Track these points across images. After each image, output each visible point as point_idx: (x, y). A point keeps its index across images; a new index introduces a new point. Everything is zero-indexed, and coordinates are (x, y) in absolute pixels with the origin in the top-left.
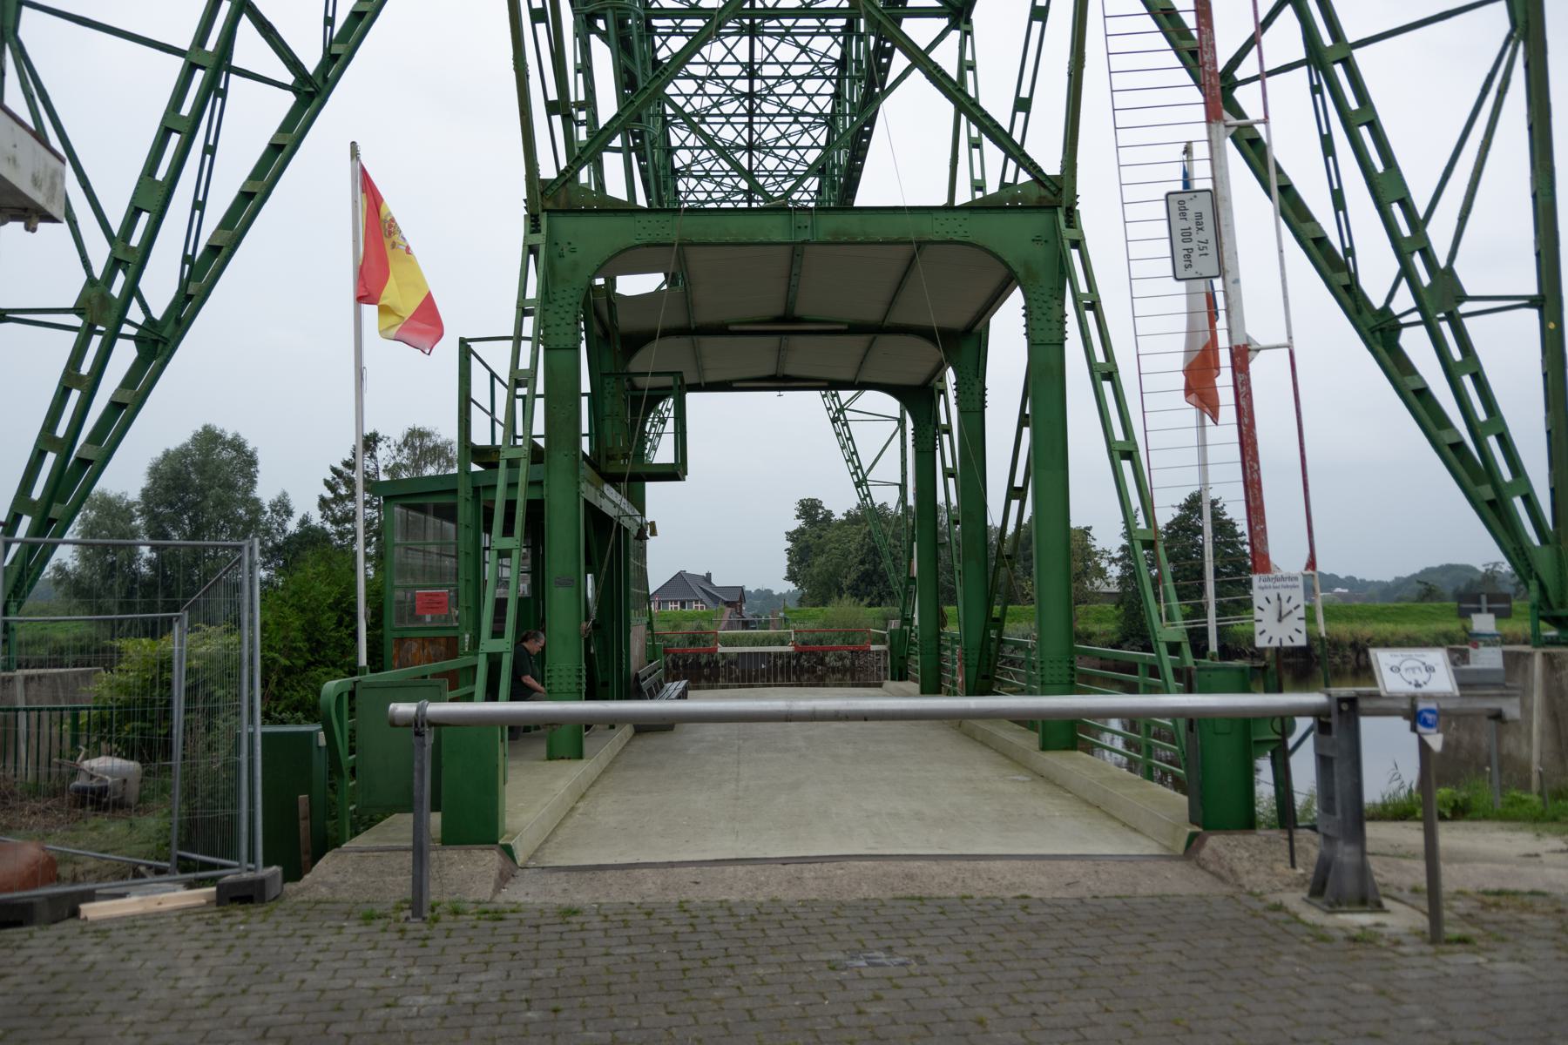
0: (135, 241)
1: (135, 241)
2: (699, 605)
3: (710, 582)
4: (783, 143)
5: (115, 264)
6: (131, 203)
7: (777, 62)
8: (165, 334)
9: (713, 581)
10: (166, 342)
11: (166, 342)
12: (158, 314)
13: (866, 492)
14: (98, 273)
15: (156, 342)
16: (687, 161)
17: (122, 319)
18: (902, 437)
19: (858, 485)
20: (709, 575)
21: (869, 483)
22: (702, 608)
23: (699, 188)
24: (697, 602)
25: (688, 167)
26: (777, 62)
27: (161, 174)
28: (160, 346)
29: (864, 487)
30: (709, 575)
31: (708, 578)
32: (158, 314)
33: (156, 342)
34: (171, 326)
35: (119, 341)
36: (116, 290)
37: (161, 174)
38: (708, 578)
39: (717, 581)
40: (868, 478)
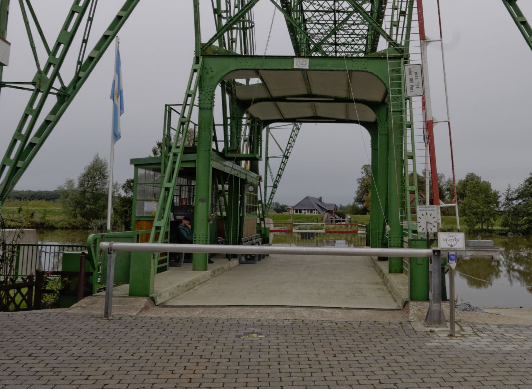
0: (58, 56)
1: (58, 56)
2: (316, 212)
3: (321, 202)
5: (49, 65)
6: (57, 41)
8: (69, 93)
9: (322, 201)
10: (69, 96)
11: (69, 96)
12: (66, 84)
14: (42, 68)
15: (65, 96)
16: (310, 16)
17: (50, 87)
20: (321, 198)
22: (317, 213)
23: (315, 27)
24: (314, 210)
25: (309, 18)
27: (70, 29)
28: (66, 98)
30: (321, 198)
31: (320, 200)
32: (66, 84)
33: (65, 96)
34: (71, 89)
35: (49, 95)
36: (49, 75)
37: (70, 29)
38: (320, 200)
39: (325, 200)
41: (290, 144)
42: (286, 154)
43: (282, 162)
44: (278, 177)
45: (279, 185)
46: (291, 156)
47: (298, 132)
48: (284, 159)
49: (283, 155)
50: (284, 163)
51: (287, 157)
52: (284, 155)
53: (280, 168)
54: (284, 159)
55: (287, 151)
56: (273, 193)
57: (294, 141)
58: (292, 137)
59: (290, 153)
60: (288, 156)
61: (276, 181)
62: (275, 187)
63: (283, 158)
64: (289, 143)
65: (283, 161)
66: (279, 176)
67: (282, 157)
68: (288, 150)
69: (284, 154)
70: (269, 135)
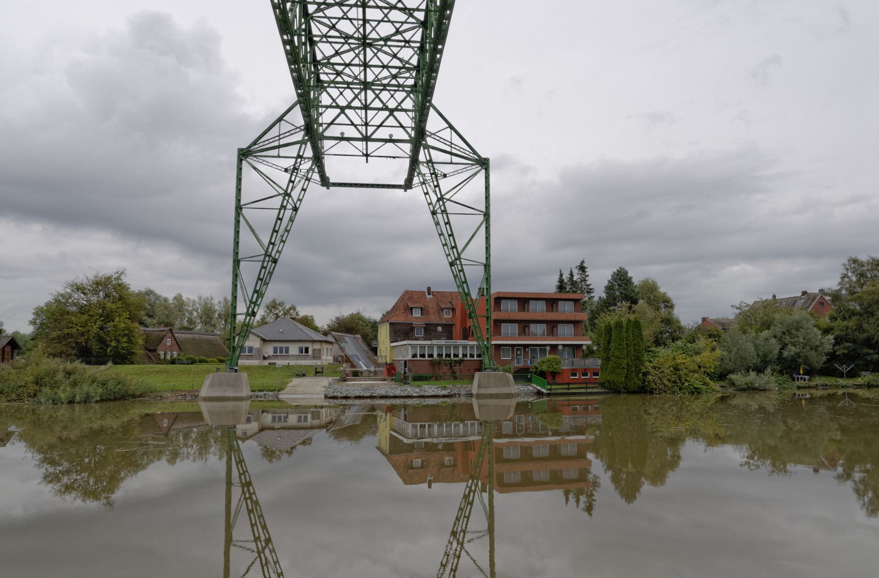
4: (394, 71)
7: (392, 22)
13: (460, 268)
18: (486, 228)
19: (452, 264)
21: (463, 262)
26: (392, 22)
29: (459, 267)
40: (461, 256)
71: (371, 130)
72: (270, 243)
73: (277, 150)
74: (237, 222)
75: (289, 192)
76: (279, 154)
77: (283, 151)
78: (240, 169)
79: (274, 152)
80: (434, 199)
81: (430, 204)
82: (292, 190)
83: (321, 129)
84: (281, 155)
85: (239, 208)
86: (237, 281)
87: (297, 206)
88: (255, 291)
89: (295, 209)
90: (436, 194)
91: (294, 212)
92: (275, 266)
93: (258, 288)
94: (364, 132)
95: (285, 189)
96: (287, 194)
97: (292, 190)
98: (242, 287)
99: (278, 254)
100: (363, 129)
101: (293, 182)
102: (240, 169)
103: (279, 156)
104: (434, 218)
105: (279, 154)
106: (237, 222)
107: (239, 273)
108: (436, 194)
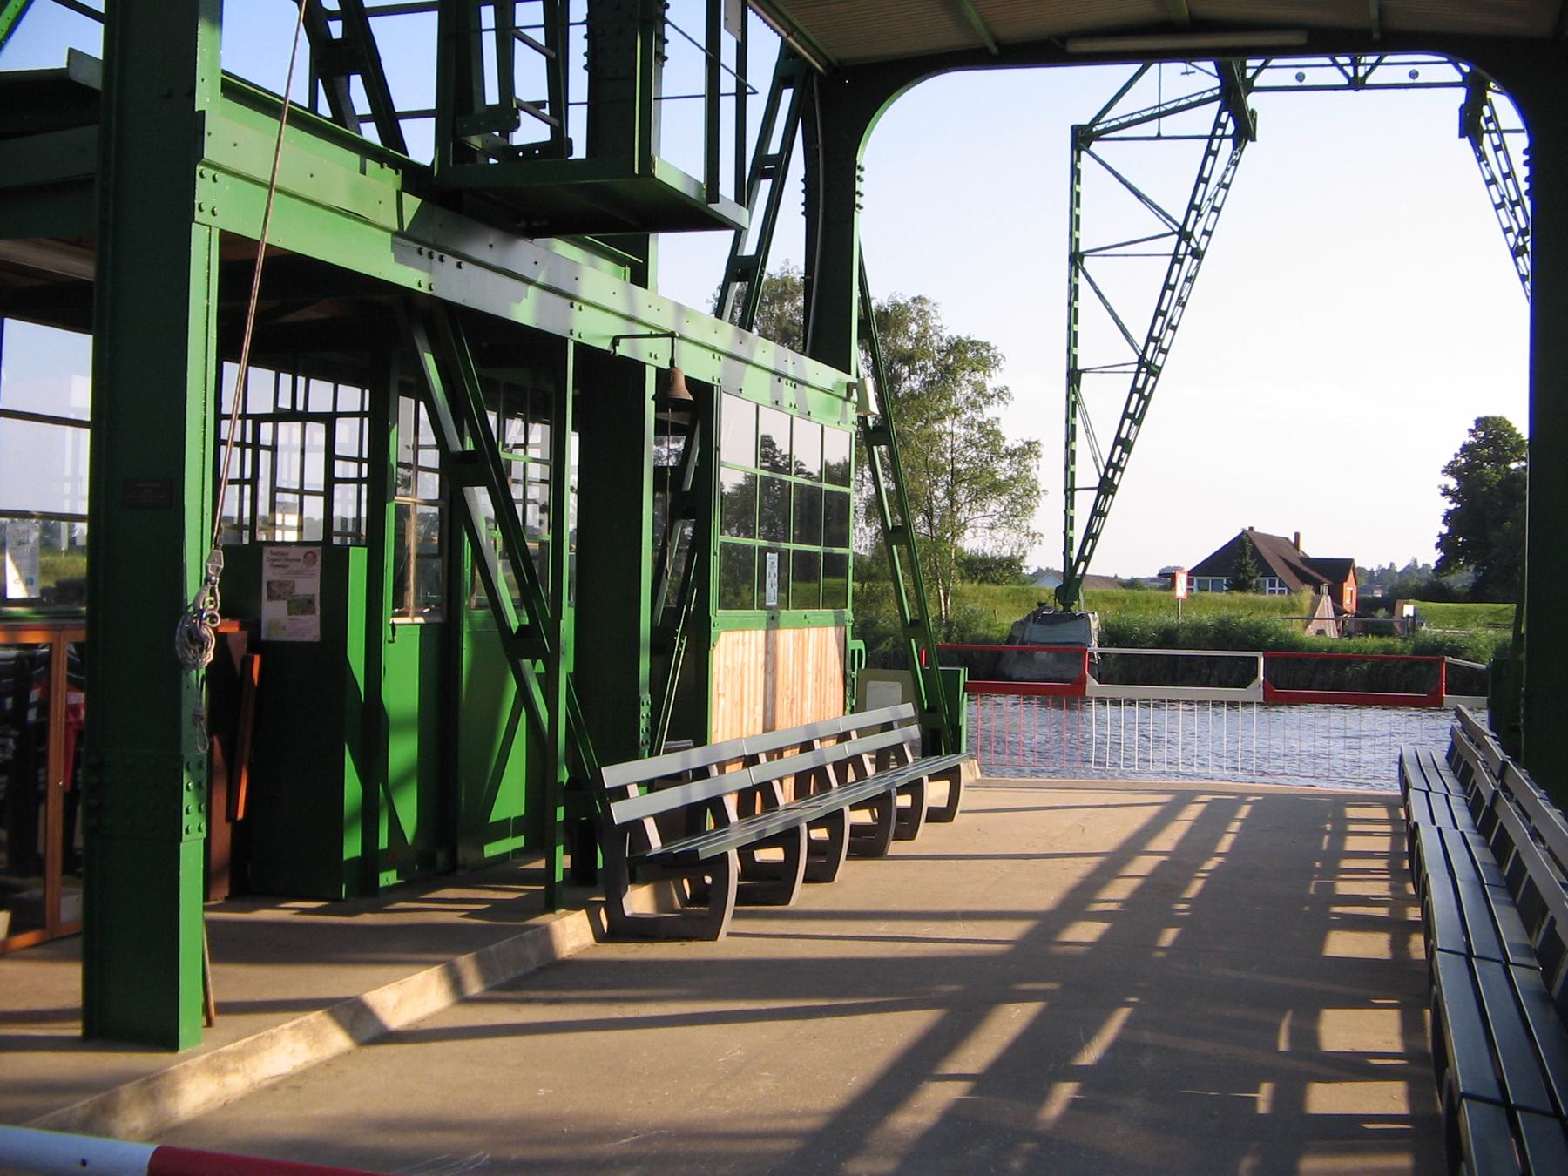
41: (1164, 314)
42: (1148, 356)
43: (1134, 390)
44: (1119, 448)
45: (1126, 483)
46: (1171, 367)
47: (1198, 267)
48: (1142, 377)
49: (1136, 359)
50: (1141, 391)
51: (1154, 371)
52: (1142, 362)
53: (1126, 415)
54: (1142, 377)
55: (1152, 345)
56: (1098, 513)
57: (1182, 303)
58: (1173, 288)
59: (1166, 352)
60: (1159, 363)
61: (1110, 464)
62: (1106, 488)
63: (1138, 373)
64: (1159, 312)
65: (1139, 384)
66: (1124, 444)
67: (1135, 367)
68: (1157, 340)
69: (1142, 357)
70: (1082, 281)
71: (1361, 71)
72: (1150, 338)
73: (1157, 120)
74: (1074, 291)
75: (1189, 228)
76: (1159, 134)
77: (1169, 125)
78: (1075, 174)
79: (1149, 129)
80: (1516, 230)
81: (1507, 231)
82: (1196, 222)
83: (1249, 73)
84: (1163, 134)
85: (1076, 259)
86: (1074, 415)
87: (1202, 248)
88: (1118, 440)
89: (1197, 254)
90: (1516, 218)
91: (1196, 261)
92: (1154, 385)
93: (1123, 435)
94: (1352, 75)
95: (1181, 223)
96: (1184, 235)
97: (1196, 222)
98: (1087, 431)
99: (1161, 356)
100: (1350, 70)
101: (1198, 208)
102: (1075, 174)
103: (1159, 137)
104: (1517, 264)
105: (1159, 134)
106: (1074, 291)
107: (1080, 401)
108: (1516, 218)
